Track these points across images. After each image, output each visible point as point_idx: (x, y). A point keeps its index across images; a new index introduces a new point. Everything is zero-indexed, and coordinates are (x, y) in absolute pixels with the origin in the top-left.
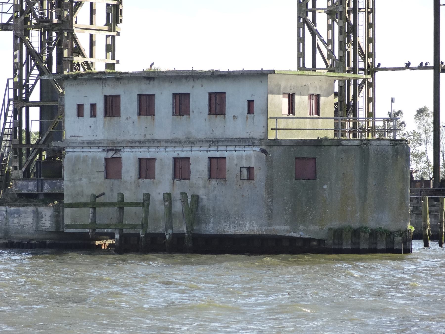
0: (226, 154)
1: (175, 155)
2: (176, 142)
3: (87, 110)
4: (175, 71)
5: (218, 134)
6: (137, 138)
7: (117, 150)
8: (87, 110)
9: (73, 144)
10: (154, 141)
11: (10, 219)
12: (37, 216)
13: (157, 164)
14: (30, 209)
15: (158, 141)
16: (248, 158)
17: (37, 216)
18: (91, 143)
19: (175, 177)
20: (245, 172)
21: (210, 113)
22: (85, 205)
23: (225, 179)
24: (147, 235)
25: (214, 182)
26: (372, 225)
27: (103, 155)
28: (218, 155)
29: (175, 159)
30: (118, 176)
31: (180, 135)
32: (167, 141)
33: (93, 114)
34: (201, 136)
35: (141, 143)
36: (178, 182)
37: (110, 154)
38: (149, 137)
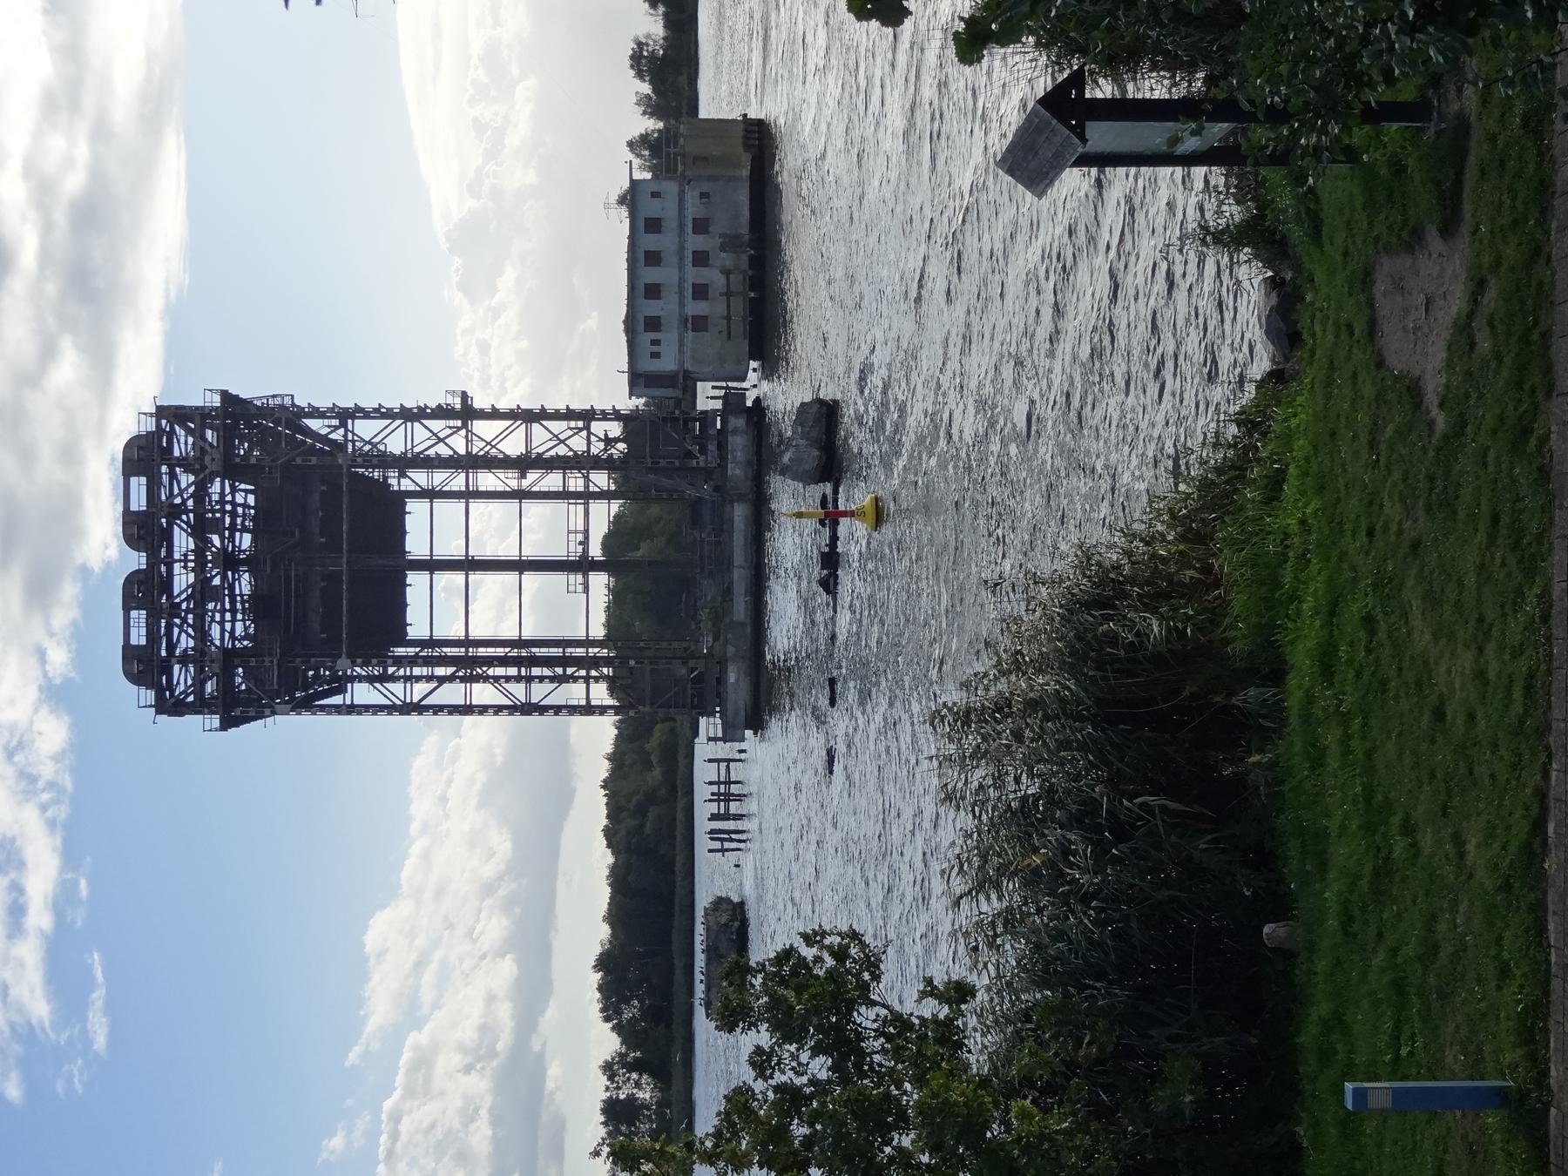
0: (690, 218)
1: (691, 265)
2: (681, 267)
3: (655, 349)
4: (628, 269)
5: (674, 224)
6: (677, 300)
7: (687, 319)
8: (655, 349)
9: (681, 363)
10: (680, 283)
11: (738, 459)
12: (735, 432)
13: (698, 282)
14: (730, 438)
15: (680, 279)
16: (693, 197)
17: (735, 432)
18: (681, 344)
19: (707, 265)
20: (704, 200)
21: (659, 232)
22: (728, 280)
23: (707, 219)
24: (750, 268)
25: (711, 229)
26: (741, 134)
27: (690, 331)
28: (690, 225)
29: (693, 266)
30: (706, 317)
31: (675, 260)
32: (680, 271)
33: (655, 342)
34: (676, 240)
35: (681, 294)
36: (711, 262)
37: (689, 325)
38: (677, 289)
